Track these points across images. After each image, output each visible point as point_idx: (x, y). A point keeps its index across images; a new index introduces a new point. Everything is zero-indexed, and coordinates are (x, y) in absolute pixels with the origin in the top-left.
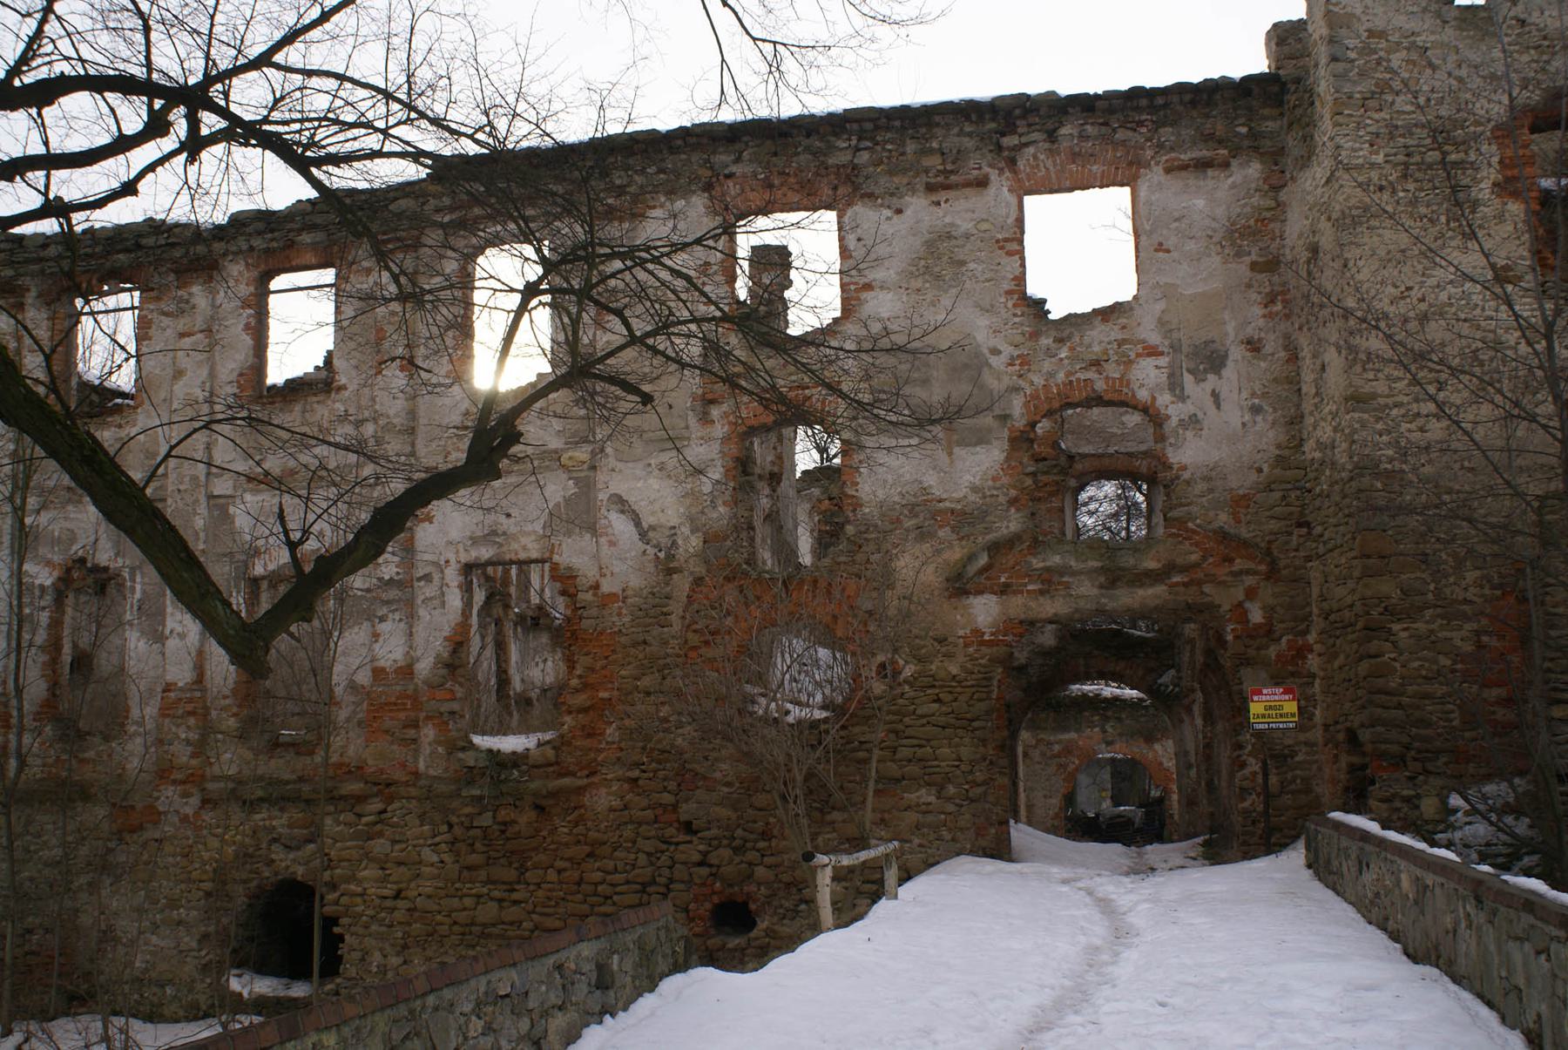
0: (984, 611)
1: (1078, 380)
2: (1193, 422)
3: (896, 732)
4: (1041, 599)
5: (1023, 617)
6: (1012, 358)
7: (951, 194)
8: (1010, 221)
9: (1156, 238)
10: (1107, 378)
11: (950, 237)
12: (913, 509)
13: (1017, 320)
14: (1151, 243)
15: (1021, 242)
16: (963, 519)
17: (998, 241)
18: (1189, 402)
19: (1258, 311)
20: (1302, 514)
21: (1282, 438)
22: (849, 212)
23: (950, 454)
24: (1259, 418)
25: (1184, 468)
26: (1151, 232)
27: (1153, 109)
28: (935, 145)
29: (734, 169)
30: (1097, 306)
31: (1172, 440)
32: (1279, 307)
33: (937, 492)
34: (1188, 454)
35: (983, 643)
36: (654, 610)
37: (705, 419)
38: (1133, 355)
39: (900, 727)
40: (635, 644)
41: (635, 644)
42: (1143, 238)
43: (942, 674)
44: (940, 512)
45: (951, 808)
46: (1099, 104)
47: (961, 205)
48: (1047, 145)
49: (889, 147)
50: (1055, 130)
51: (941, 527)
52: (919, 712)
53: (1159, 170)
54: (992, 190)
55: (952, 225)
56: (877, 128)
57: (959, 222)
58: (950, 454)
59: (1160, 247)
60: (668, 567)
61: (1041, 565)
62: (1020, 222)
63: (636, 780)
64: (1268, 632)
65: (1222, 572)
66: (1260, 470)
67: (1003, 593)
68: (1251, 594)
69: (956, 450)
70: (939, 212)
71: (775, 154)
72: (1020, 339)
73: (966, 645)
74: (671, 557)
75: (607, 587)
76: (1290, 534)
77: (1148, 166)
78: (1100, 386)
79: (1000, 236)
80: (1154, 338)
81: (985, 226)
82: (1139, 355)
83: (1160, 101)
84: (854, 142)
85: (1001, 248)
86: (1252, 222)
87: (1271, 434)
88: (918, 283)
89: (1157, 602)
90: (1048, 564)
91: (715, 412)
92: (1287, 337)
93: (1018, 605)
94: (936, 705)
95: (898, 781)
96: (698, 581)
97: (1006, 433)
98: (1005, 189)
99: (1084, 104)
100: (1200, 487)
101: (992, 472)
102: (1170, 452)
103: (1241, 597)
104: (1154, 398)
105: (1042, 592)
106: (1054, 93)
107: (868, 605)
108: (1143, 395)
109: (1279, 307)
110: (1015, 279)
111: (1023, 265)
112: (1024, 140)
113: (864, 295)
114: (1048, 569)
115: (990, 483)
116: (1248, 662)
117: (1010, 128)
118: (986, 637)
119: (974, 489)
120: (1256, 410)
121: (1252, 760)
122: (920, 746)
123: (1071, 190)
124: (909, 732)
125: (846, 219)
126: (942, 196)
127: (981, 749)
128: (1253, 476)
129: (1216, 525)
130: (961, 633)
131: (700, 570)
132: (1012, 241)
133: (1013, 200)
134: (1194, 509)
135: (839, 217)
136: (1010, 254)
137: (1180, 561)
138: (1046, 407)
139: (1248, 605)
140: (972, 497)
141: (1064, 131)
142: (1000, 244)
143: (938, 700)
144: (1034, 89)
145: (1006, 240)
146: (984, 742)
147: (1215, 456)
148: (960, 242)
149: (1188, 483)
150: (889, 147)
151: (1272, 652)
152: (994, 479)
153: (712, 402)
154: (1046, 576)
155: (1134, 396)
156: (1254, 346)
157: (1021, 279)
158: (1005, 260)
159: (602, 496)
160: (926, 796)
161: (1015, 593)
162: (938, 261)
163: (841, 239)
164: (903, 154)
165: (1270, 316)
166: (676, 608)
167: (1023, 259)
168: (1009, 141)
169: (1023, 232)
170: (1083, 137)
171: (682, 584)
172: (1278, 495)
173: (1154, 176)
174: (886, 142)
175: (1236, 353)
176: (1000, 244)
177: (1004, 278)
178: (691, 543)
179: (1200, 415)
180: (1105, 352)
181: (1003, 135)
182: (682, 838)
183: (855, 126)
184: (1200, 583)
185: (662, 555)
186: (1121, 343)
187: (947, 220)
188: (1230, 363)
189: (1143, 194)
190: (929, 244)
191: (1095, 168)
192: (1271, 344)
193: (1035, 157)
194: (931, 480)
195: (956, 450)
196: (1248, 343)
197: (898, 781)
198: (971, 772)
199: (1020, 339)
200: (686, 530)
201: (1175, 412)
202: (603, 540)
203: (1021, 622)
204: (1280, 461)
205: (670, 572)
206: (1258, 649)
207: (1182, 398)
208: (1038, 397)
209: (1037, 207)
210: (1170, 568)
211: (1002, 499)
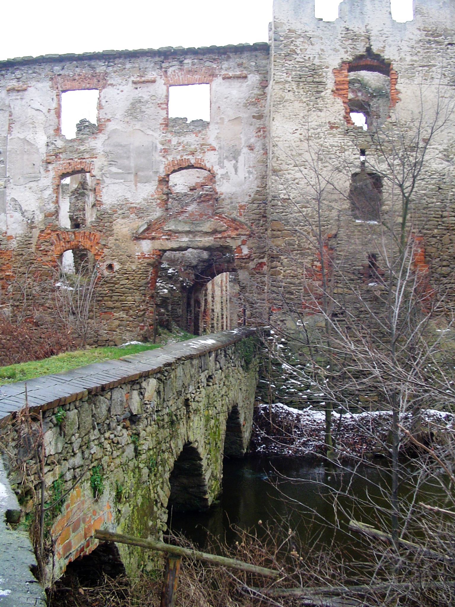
0: (146, 247)
2: (226, 176)
3: (112, 290)
8: (163, 96)
9: (217, 105)
10: (196, 158)
11: (140, 102)
12: (121, 206)
13: (164, 135)
15: (167, 104)
16: (139, 212)
17: (158, 104)
19: (254, 134)
20: (265, 213)
21: (259, 184)
22: (104, 91)
23: (136, 186)
24: (251, 176)
25: (222, 194)
26: (215, 102)
29: (61, 72)
31: (218, 183)
32: (262, 133)
33: (131, 200)
34: (224, 188)
35: (145, 258)
36: (26, 243)
37: (47, 171)
38: (206, 150)
40: (19, 255)
41: (19, 255)
42: (212, 105)
43: (130, 269)
44: (131, 208)
45: (131, 319)
47: (145, 89)
48: (179, 67)
50: (183, 61)
51: (131, 213)
52: (120, 283)
54: (157, 83)
55: (142, 97)
57: (144, 96)
58: (136, 186)
60: (31, 226)
61: (168, 229)
62: (167, 97)
64: (249, 258)
65: (233, 234)
66: (250, 196)
68: (244, 243)
69: (139, 184)
71: (77, 67)
73: (139, 258)
74: (33, 222)
75: (8, 234)
76: (260, 220)
77: (216, 76)
78: (193, 161)
79: (159, 102)
80: (215, 144)
82: (208, 150)
83: (222, 51)
85: (159, 107)
86: (254, 100)
87: (256, 182)
88: (127, 119)
89: (210, 244)
90: (170, 229)
92: (264, 145)
93: (158, 244)
94: (127, 281)
95: (112, 308)
96: (42, 231)
97: (157, 179)
100: (228, 201)
101: (151, 193)
102: (217, 188)
103: (240, 244)
104: (213, 167)
105: (167, 239)
107: (103, 243)
108: (208, 166)
109: (262, 133)
112: (170, 64)
113: (107, 123)
115: (150, 197)
116: (241, 268)
118: (146, 256)
119: (145, 200)
120: (250, 172)
124: (117, 290)
125: (102, 93)
127: (143, 298)
128: (247, 199)
129: (232, 216)
130: (137, 254)
131: (43, 227)
133: (165, 87)
134: (225, 209)
136: (162, 109)
137: (219, 229)
138: (173, 169)
139: (242, 247)
140: (143, 202)
141: (186, 61)
143: (128, 279)
145: (161, 104)
146: (145, 295)
147: (234, 190)
149: (223, 200)
152: (152, 196)
153: (49, 163)
154: (169, 233)
155: (205, 165)
156: (251, 148)
159: (8, 198)
160: (122, 314)
165: (258, 137)
166: (34, 241)
167: (168, 111)
168: (164, 65)
169: (168, 101)
170: (193, 64)
171: (36, 233)
172: (256, 205)
174: (118, 64)
175: (245, 150)
176: (159, 105)
178: (39, 217)
180: (196, 148)
181: (163, 62)
182: (34, 328)
183: (107, 57)
184: (225, 238)
185: (29, 221)
186: (202, 145)
187: (140, 95)
188: (242, 154)
190: (132, 104)
192: (258, 147)
193: (174, 71)
194: (128, 195)
195: (139, 184)
196: (249, 147)
197: (112, 308)
198: (139, 306)
200: (37, 212)
201: (219, 172)
202: (8, 215)
203: (160, 250)
204: (257, 192)
205: (32, 228)
207: (222, 167)
210: (215, 232)
211: (154, 204)
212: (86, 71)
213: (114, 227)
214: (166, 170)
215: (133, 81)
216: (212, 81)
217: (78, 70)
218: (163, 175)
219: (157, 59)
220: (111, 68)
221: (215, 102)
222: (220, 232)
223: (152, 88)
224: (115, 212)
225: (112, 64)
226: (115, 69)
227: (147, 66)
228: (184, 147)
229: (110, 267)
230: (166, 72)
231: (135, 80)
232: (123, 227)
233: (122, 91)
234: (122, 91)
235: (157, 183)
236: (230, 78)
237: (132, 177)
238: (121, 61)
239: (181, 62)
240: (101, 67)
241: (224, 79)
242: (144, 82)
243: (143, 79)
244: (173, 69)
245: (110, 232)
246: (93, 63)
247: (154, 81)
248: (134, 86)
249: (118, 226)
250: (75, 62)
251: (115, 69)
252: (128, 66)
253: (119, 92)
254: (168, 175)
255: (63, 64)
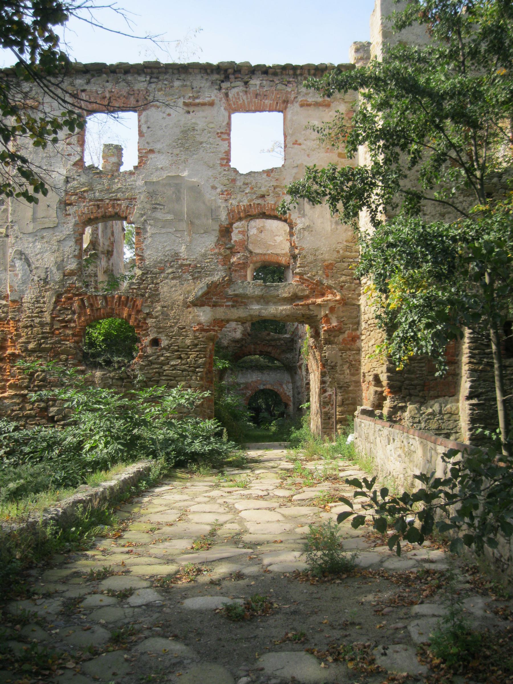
0: (204, 315)
1: (254, 204)
4: (232, 310)
5: (223, 318)
6: (222, 191)
7: (196, 109)
14: (291, 140)
15: (229, 135)
18: (307, 218)
22: (144, 113)
26: (292, 135)
27: (295, 75)
28: (188, 83)
29: (86, 87)
30: (265, 169)
39: (161, 370)
42: (288, 137)
46: (270, 71)
48: (244, 89)
49: (166, 82)
53: (297, 105)
54: (216, 108)
56: (159, 73)
57: (199, 122)
59: (296, 143)
62: (229, 124)
63: (24, 396)
66: (338, 252)
67: (214, 306)
70: (189, 116)
71: (108, 81)
72: (226, 182)
81: (212, 125)
84: (148, 79)
85: (220, 137)
88: (176, 151)
89: (288, 313)
90: (236, 292)
91: (71, 210)
93: (221, 312)
97: (217, 227)
98: (222, 108)
99: (264, 71)
105: (233, 306)
106: (248, 63)
110: (226, 152)
111: (229, 146)
112: (233, 85)
113: (151, 156)
114: (236, 295)
117: (227, 78)
118: (205, 328)
121: (329, 389)
122: (171, 380)
123: (255, 111)
125: (142, 116)
126: (191, 109)
128: (335, 255)
132: (225, 134)
133: (226, 114)
135: (139, 116)
136: (223, 140)
137: (300, 294)
139: (330, 316)
141: (252, 82)
142: (219, 135)
143: (180, 358)
144: (238, 61)
145: (222, 133)
148: (199, 132)
150: (166, 82)
151: (341, 338)
157: (228, 153)
158: (221, 143)
161: (220, 306)
162: (187, 142)
163: (140, 127)
164: (172, 87)
167: (229, 143)
168: (224, 85)
169: (230, 130)
170: (261, 86)
173: (294, 109)
174: (164, 80)
176: (219, 135)
177: (220, 152)
179: (312, 225)
183: (149, 71)
187: (193, 121)
189: (289, 116)
190: (184, 132)
191: (266, 101)
193: (238, 94)
199: (226, 182)
206: (335, 337)
208: (234, 211)
209: (238, 119)
212: (122, 89)
213: (161, 290)
214: (229, 218)
215: (184, 102)
216: (286, 108)
217: (109, 86)
218: (225, 223)
219: (215, 77)
220: (153, 86)
221: (292, 135)
222: (301, 298)
223: (208, 112)
224: (162, 271)
225: (155, 80)
226: (159, 86)
227: (202, 85)
228: (252, 188)
229: (155, 342)
230: (227, 95)
231: (187, 101)
232: (174, 292)
233: (169, 115)
234: (169, 115)
235: (217, 233)
236: (309, 105)
237: (183, 226)
238: (167, 76)
239: (246, 83)
240: (141, 83)
241: (302, 106)
242: (198, 105)
243: (197, 101)
244: (236, 90)
245: (155, 296)
246: (129, 78)
247: (212, 104)
248: (186, 108)
249: (165, 289)
250: (104, 75)
251: (159, 86)
252: (177, 83)
253: (165, 115)
254: (231, 224)
255: (88, 76)
